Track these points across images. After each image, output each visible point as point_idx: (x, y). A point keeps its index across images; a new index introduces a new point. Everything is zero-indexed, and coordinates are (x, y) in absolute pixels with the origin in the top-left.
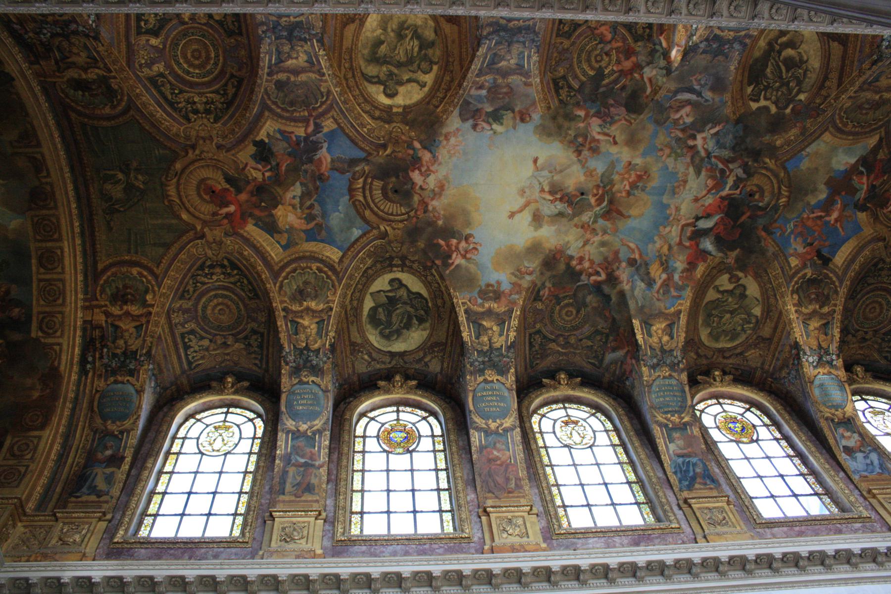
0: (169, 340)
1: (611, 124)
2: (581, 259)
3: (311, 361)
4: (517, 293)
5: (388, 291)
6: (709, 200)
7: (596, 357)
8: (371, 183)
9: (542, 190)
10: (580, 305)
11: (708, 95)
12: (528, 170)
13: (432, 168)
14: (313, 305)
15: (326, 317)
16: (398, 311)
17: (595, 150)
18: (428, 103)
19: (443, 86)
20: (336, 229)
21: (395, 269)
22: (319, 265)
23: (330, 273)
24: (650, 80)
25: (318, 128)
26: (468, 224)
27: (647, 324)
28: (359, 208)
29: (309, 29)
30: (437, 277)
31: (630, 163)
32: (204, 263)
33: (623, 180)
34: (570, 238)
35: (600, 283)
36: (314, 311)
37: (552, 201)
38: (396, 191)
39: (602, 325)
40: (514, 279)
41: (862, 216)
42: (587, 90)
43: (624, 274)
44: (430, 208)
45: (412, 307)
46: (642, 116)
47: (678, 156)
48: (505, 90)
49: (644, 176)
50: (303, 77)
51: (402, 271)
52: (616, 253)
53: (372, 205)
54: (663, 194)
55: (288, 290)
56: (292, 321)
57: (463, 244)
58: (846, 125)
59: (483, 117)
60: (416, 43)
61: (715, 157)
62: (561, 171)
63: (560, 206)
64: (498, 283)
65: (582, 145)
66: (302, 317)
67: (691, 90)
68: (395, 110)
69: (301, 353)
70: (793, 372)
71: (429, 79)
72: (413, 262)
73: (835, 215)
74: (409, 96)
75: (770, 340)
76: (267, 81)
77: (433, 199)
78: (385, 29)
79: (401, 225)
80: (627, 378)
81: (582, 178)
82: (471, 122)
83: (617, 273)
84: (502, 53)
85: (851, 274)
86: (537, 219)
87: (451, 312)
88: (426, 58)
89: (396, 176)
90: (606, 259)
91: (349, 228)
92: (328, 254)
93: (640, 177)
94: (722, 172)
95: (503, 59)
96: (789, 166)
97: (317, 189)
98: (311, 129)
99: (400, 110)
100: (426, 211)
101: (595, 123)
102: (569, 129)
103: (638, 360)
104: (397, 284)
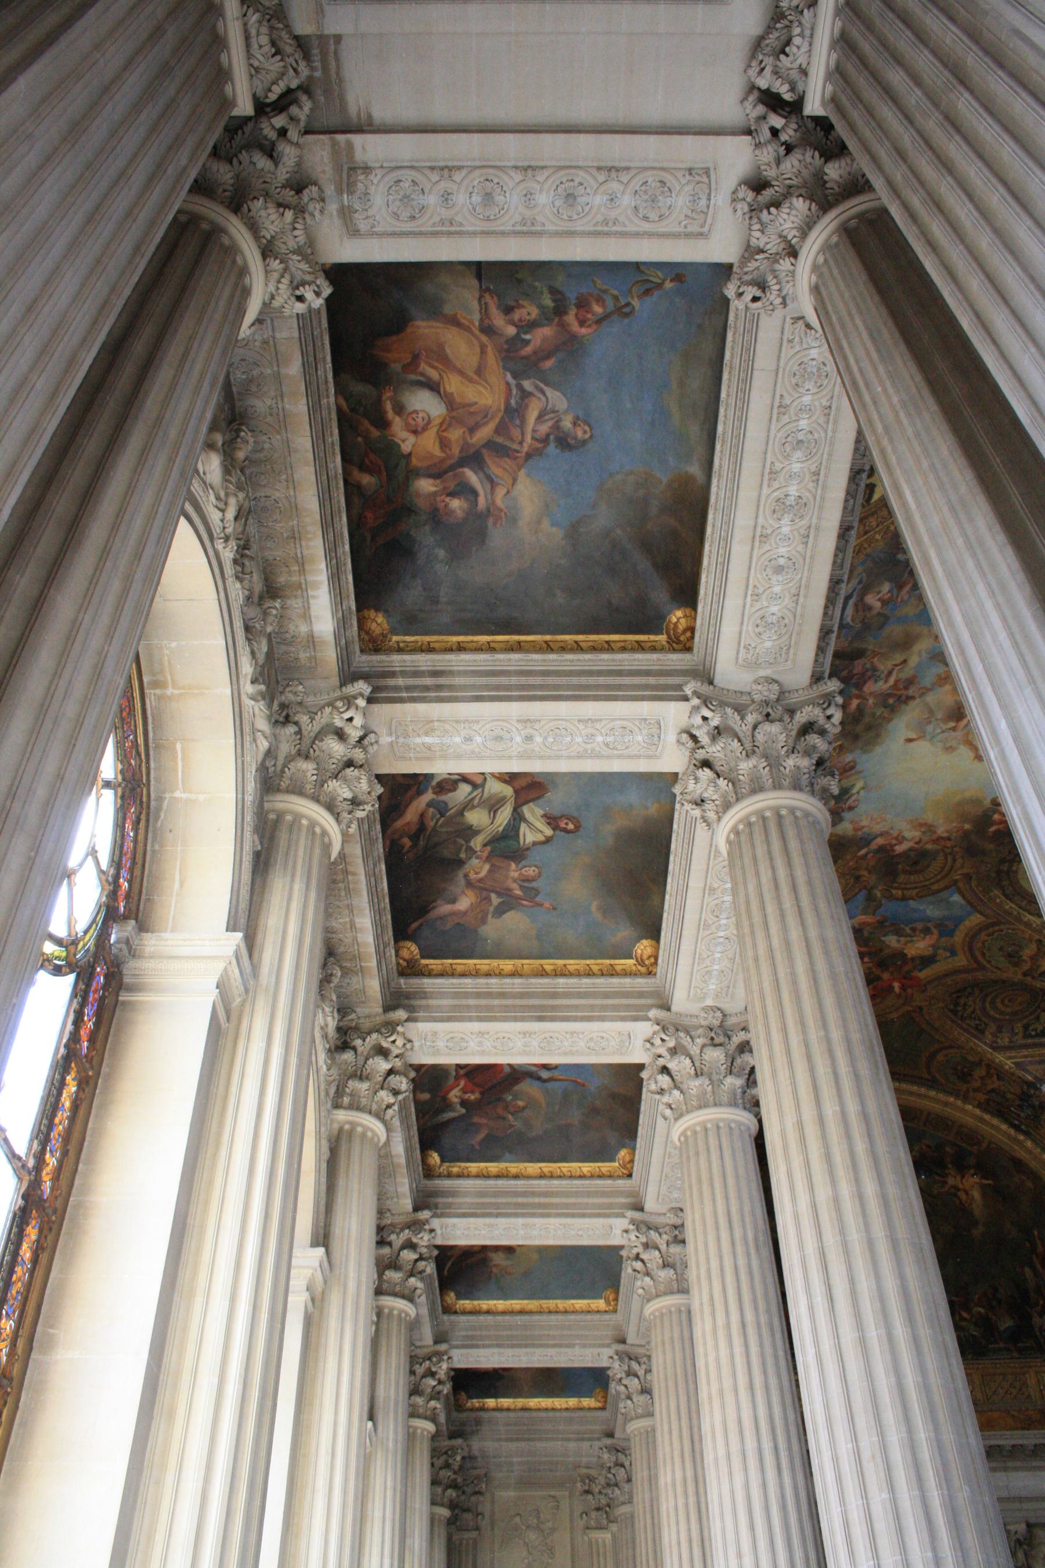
0: (1025, 1052)
1: (875, 669)
9: (954, 729)
12: (923, 747)
13: (895, 833)
17: (910, 682)
20: (946, 913)
26: (976, 802)
28: (925, 892)
32: (951, 1011)
44: (945, 835)
46: (871, 647)
62: (931, 712)
100: (949, 839)
101: (870, 687)
102: (873, 715)
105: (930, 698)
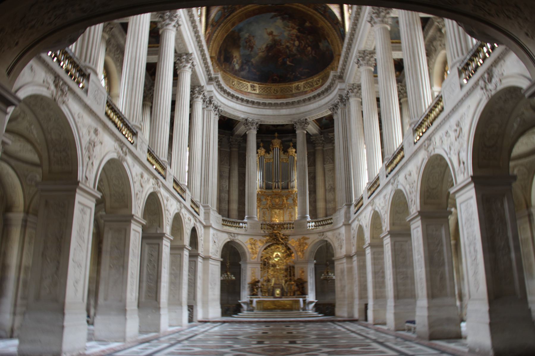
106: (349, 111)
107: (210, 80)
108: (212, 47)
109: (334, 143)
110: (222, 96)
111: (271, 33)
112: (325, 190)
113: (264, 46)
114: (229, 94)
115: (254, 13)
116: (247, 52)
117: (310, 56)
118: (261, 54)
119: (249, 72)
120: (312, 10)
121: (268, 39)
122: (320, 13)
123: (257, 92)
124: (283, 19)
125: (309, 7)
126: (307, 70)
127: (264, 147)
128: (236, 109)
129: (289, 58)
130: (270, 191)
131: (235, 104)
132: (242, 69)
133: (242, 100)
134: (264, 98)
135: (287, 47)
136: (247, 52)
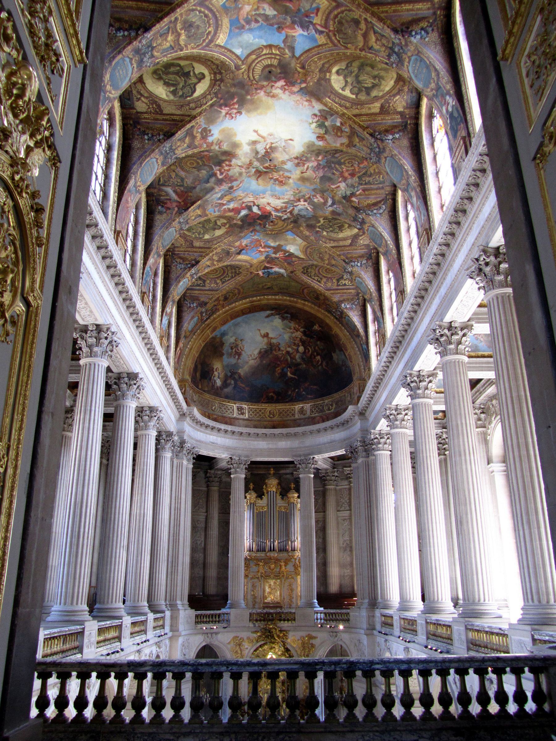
1: (314, 171)
2: (230, 166)
3: (145, 56)
4: (207, 146)
5: (194, 73)
6: (268, 208)
7: (165, 182)
8: (275, 58)
9: (272, 143)
10: (199, 169)
11: (330, 209)
13: (287, 92)
14: (183, 37)
15: (175, 49)
16: (178, 78)
17: (297, 165)
18: (332, 92)
19: (343, 102)
20: (240, 39)
21: (212, 75)
22: (213, 32)
23: (207, 41)
24: (339, 187)
25: (321, 32)
26: (248, 111)
27: (199, 207)
28: (257, 51)
29: (397, 65)
30: (211, 102)
31: (290, 178)
33: (280, 176)
34: (243, 159)
35: (215, 175)
36: (178, 40)
37: (265, 148)
38: (270, 72)
39: (189, 181)
40: (215, 142)
41: (263, 258)
42: (333, 160)
43: (225, 187)
44: (259, 91)
45: (183, 86)
47: (294, 196)
48: (339, 134)
49: (282, 183)
50: (360, 38)
51: (211, 80)
52: (236, 180)
53: (259, 59)
54: (271, 191)
55: (191, 16)
56: (169, 28)
57: (235, 111)
58: (312, 249)
59: (321, 120)
60: (370, 85)
61: (293, 209)
62: (285, 151)
63: (262, 152)
64: (212, 135)
65: (300, 160)
66: (173, 33)
67: (333, 204)
68: (328, 74)
69: (148, 47)
70: (183, 266)
71: (347, 93)
72: (219, 86)
73: (263, 250)
74: (337, 82)
75: (193, 247)
76: (360, 15)
77: (265, 92)
78: (381, 69)
79: (246, 77)
80: (162, 206)
81: (281, 160)
82: (319, 114)
83: (224, 184)
84: (364, 142)
85: (233, 263)
86: (255, 143)
87: (189, 116)
88: (360, 91)
89: (283, 72)
90: (232, 177)
91: (242, 47)
92: (221, 36)
93: (282, 182)
94: (285, 211)
95: (360, 141)
96: (289, 232)
97: (272, 25)
98: (319, 28)
99: (328, 77)
100: (256, 89)
101: (315, 164)
103: (180, 213)
104: (201, 77)
105: (287, 157)
106: (375, 463)
107: (183, 415)
108: (185, 365)
109: (350, 482)
110: (198, 430)
111: (266, 335)
112: (340, 548)
113: (256, 352)
114: (207, 426)
115: (244, 312)
116: (233, 361)
117: (320, 367)
118: (252, 362)
119: (234, 388)
120: (323, 311)
121: (262, 344)
122: (335, 317)
123: (247, 416)
124: (283, 318)
125: (319, 307)
126: (315, 387)
127: (255, 490)
128: (217, 443)
129: (290, 367)
130: (263, 554)
131: (215, 437)
132: (225, 384)
133: (226, 431)
134: (255, 427)
135: (288, 352)
136: (233, 361)
